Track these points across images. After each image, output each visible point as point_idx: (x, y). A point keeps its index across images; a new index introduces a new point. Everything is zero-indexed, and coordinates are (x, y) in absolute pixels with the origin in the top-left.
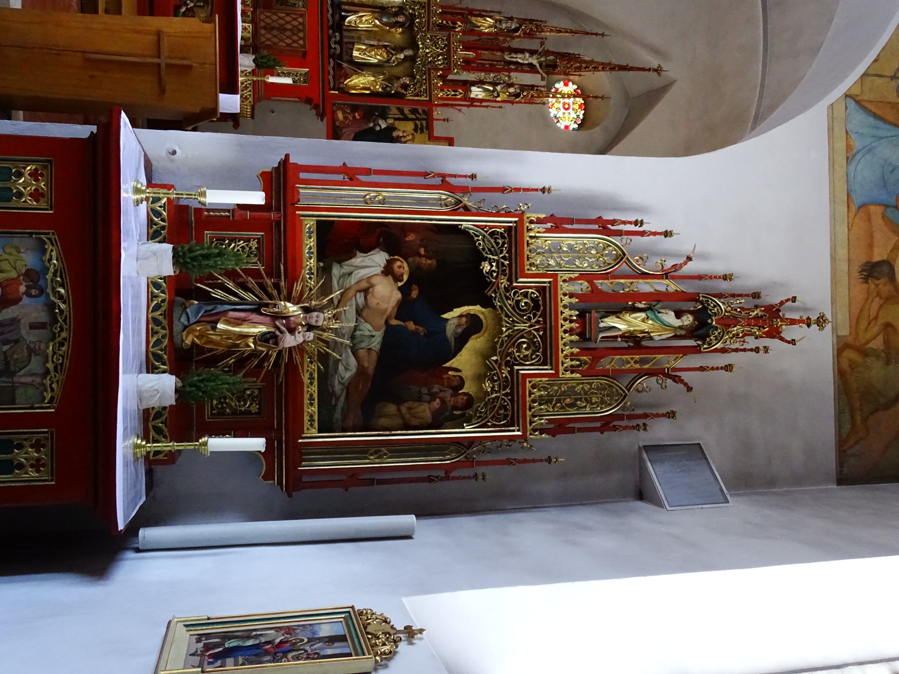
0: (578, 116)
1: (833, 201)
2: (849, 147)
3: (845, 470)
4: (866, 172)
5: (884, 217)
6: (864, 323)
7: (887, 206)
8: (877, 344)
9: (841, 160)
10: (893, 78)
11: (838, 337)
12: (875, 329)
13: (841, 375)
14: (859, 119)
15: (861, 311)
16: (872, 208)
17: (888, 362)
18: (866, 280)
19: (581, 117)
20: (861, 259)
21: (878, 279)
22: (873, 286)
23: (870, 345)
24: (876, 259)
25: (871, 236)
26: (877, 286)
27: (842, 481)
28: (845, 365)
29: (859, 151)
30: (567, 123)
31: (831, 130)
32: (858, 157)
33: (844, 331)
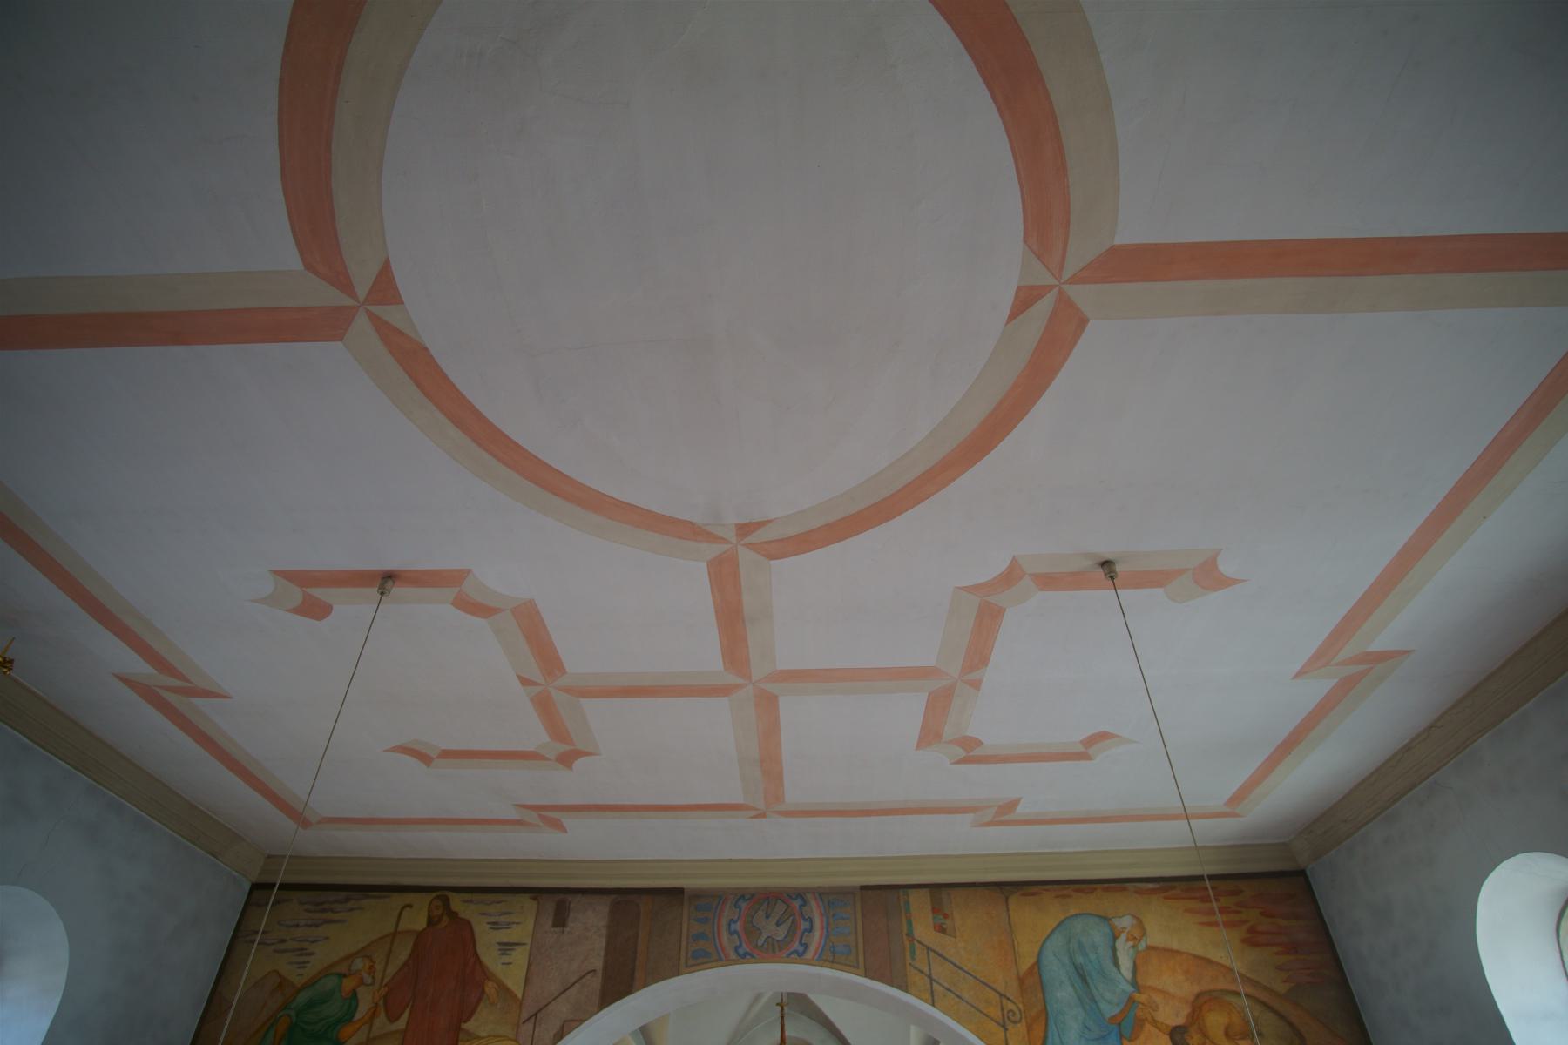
7: (1121, 1036)
10: (1004, 1026)
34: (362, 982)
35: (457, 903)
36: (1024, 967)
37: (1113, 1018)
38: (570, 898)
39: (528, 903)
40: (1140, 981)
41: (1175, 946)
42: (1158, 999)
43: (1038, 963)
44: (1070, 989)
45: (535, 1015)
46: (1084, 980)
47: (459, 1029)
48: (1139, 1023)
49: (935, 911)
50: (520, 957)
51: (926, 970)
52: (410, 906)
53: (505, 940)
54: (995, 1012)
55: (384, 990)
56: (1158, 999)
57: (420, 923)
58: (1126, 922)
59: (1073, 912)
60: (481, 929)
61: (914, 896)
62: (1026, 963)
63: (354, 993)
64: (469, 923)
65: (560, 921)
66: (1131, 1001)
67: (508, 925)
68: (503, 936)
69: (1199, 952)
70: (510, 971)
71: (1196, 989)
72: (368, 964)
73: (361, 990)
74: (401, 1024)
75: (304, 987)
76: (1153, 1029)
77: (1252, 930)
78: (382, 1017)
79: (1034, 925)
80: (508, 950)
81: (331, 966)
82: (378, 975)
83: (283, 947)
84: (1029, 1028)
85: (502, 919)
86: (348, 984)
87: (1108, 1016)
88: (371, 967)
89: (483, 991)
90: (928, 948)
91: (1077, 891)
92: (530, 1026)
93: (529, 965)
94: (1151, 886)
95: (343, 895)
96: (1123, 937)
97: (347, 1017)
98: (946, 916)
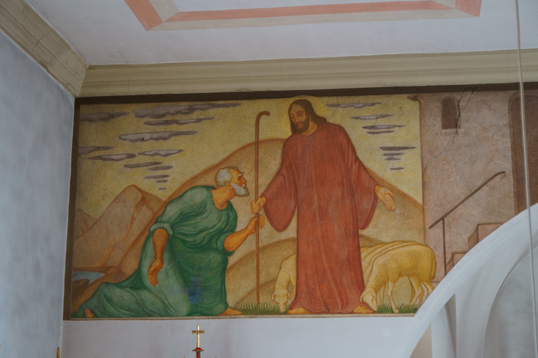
34: (234, 193)
35: (321, 107)
38: (457, 96)
39: (409, 105)
45: (443, 219)
47: (357, 236)
50: (411, 161)
52: (267, 113)
53: (390, 145)
55: (262, 201)
57: (286, 132)
60: (357, 134)
63: (229, 206)
64: (341, 129)
65: (451, 120)
67: (389, 129)
68: (386, 140)
70: (404, 176)
72: (236, 176)
73: (235, 201)
74: (291, 231)
75: (170, 201)
78: (267, 229)
80: (394, 152)
81: (196, 178)
82: (251, 186)
83: (133, 161)
85: (380, 122)
86: (220, 196)
88: (240, 178)
89: (376, 198)
92: (438, 230)
93: (424, 170)
95: (184, 105)
97: (230, 227)
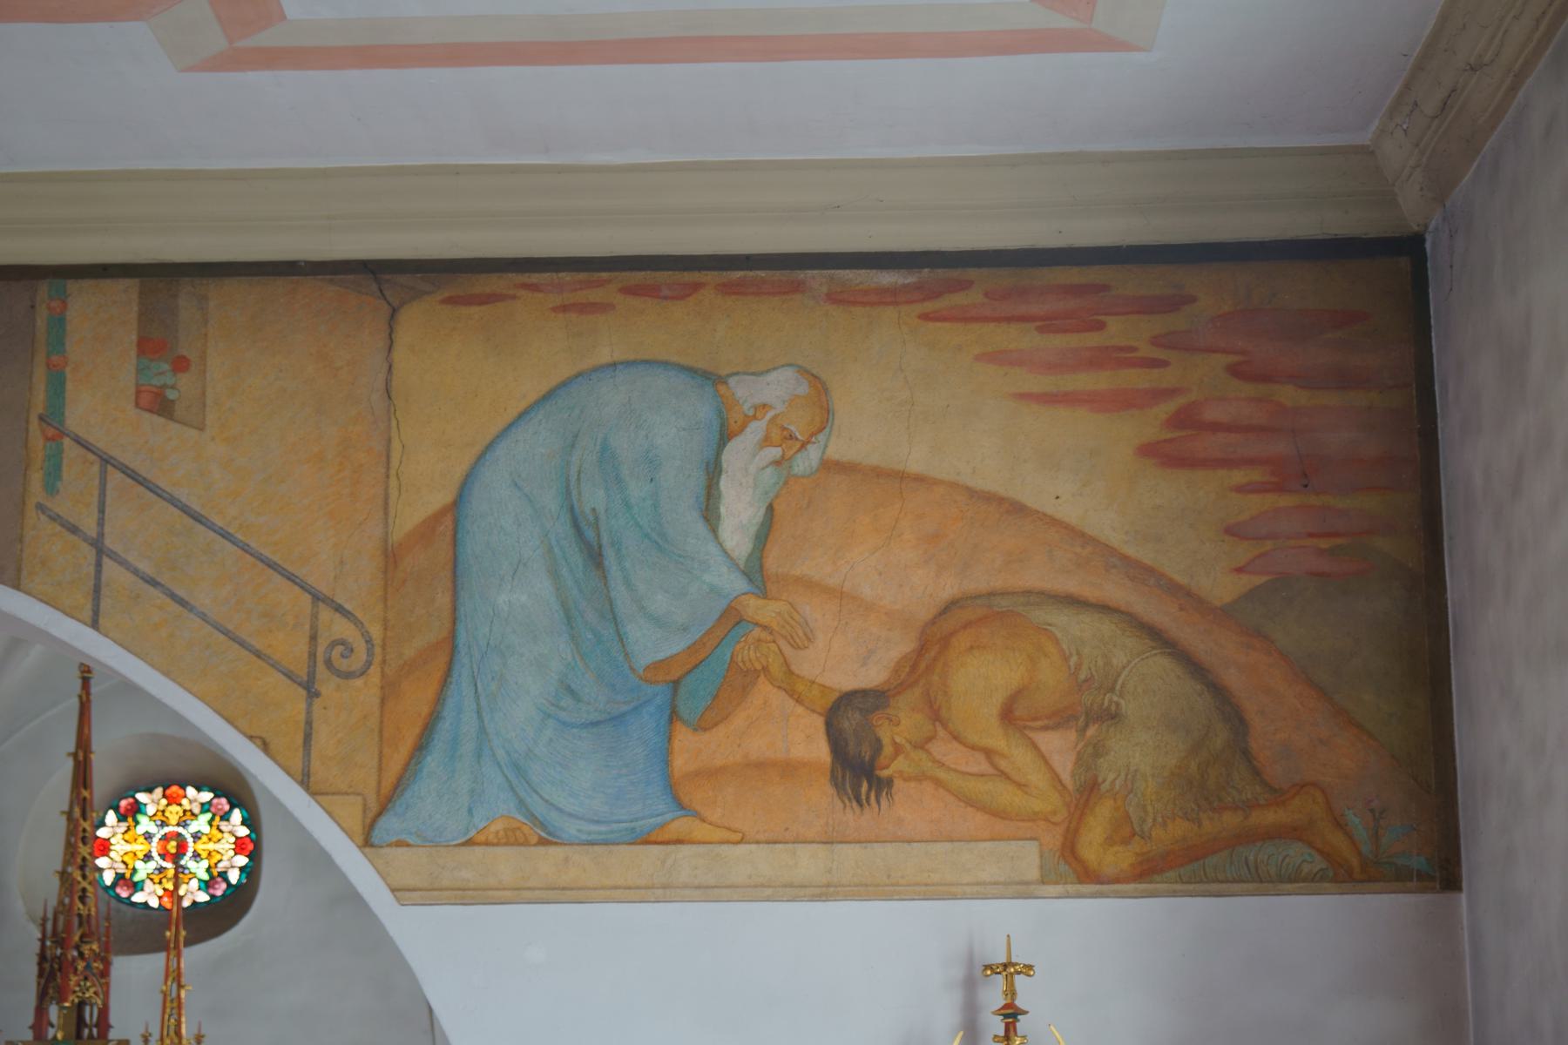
0: (205, 808)
1: (662, 891)
2: (512, 839)
3: (1418, 862)
4: (580, 784)
5: (701, 726)
6: (1006, 795)
7: (674, 716)
8: (1059, 746)
9: (546, 862)
10: (311, 690)
11: (1043, 883)
12: (1019, 757)
13: (1153, 870)
14: (432, 800)
15: (970, 802)
16: (680, 763)
17: (1112, 717)
18: (883, 786)
19: (206, 796)
20: (821, 795)
21: (878, 746)
22: (900, 764)
23: (1066, 777)
24: (821, 751)
25: (761, 766)
26: (898, 750)
27: (1443, 870)
28: (1121, 858)
29: (521, 803)
30: (227, 844)
31: (465, 895)
32: (539, 809)
33: (1027, 857)
36: (410, 515)
37: (656, 666)
40: (772, 562)
41: (916, 459)
42: (815, 612)
43: (456, 506)
44: (544, 586)
46: (595, 557)
48: (740, 680)
49: (148, 347)
51: (89, 525)
54: (292, 649)
56: (815, 612)
58: (776, 389)
59: (604, 355)
61: (83, 301)
62: (420, 503)
66: (732, 618)
69: (990, 479)
71: (949, 588)
76: (778, 698)
77: (1185, 420)
79: (461, 389)
84: (389, 691)
87: (644, 659)
90: (106, 461)
91: (727, 289)
94: (887, 278)
96: (756, 430)
98: (181, 365)
